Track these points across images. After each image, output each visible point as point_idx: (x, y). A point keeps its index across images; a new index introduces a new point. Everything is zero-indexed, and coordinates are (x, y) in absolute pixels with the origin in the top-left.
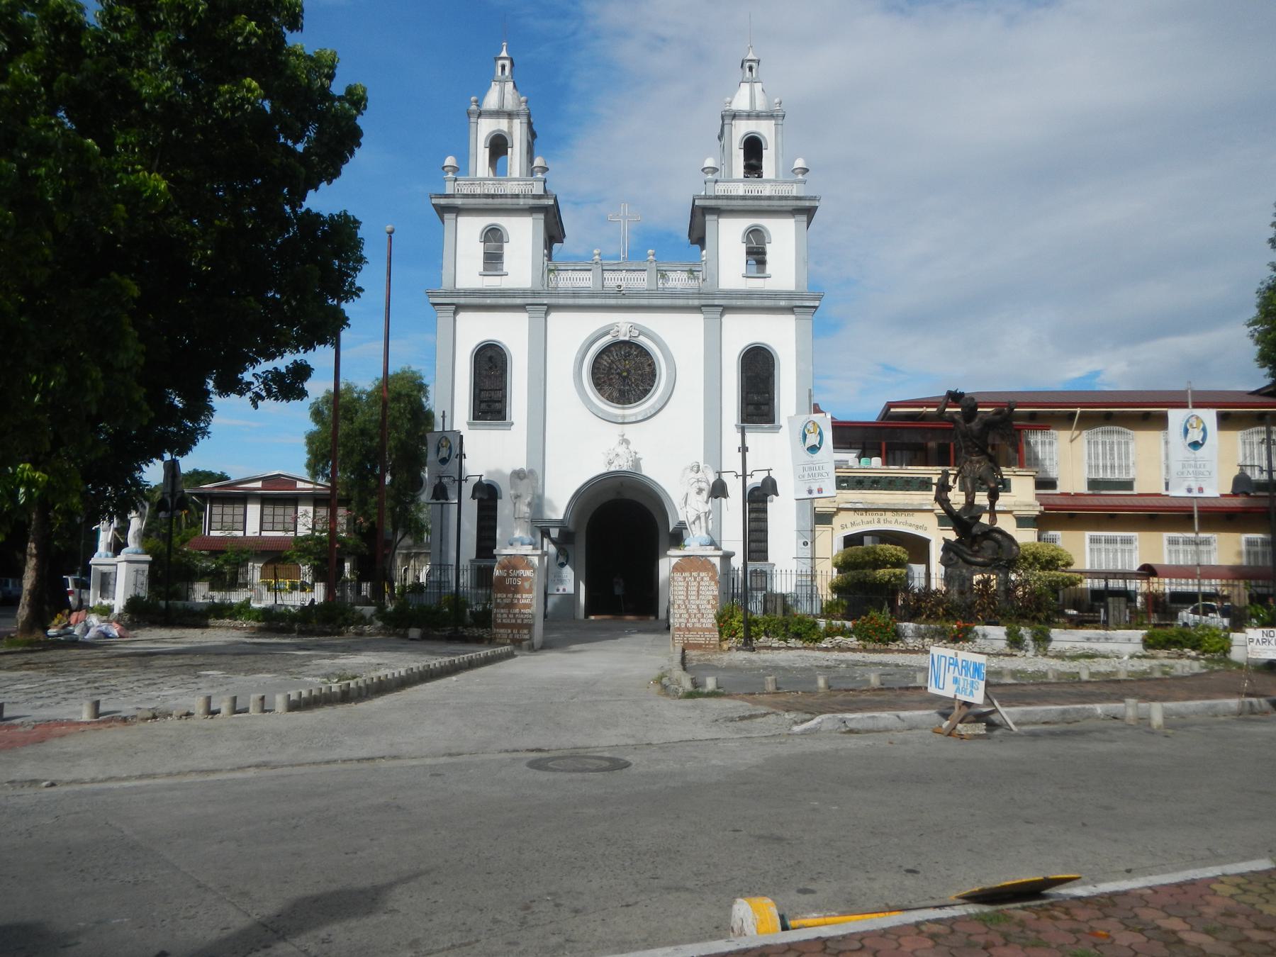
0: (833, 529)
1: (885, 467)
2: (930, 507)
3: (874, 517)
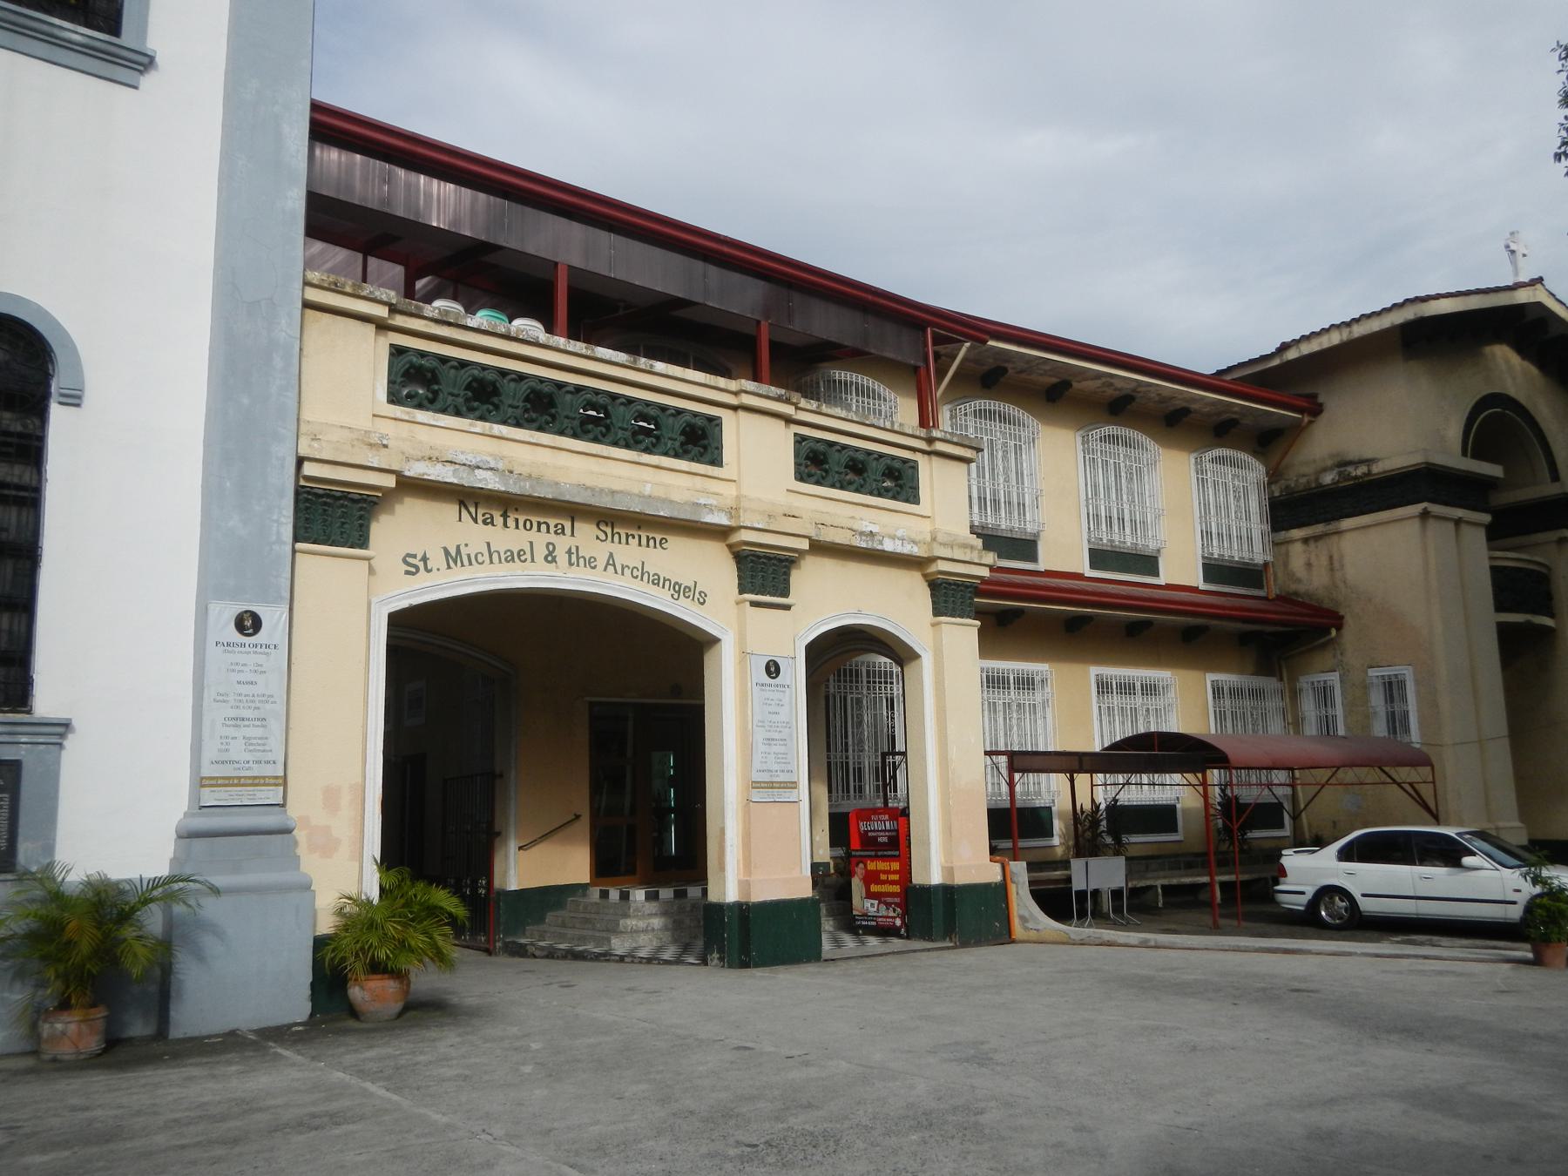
0: (371, 571)
1: (579, 347)
2: (722, 519)
3: (533, 535)
